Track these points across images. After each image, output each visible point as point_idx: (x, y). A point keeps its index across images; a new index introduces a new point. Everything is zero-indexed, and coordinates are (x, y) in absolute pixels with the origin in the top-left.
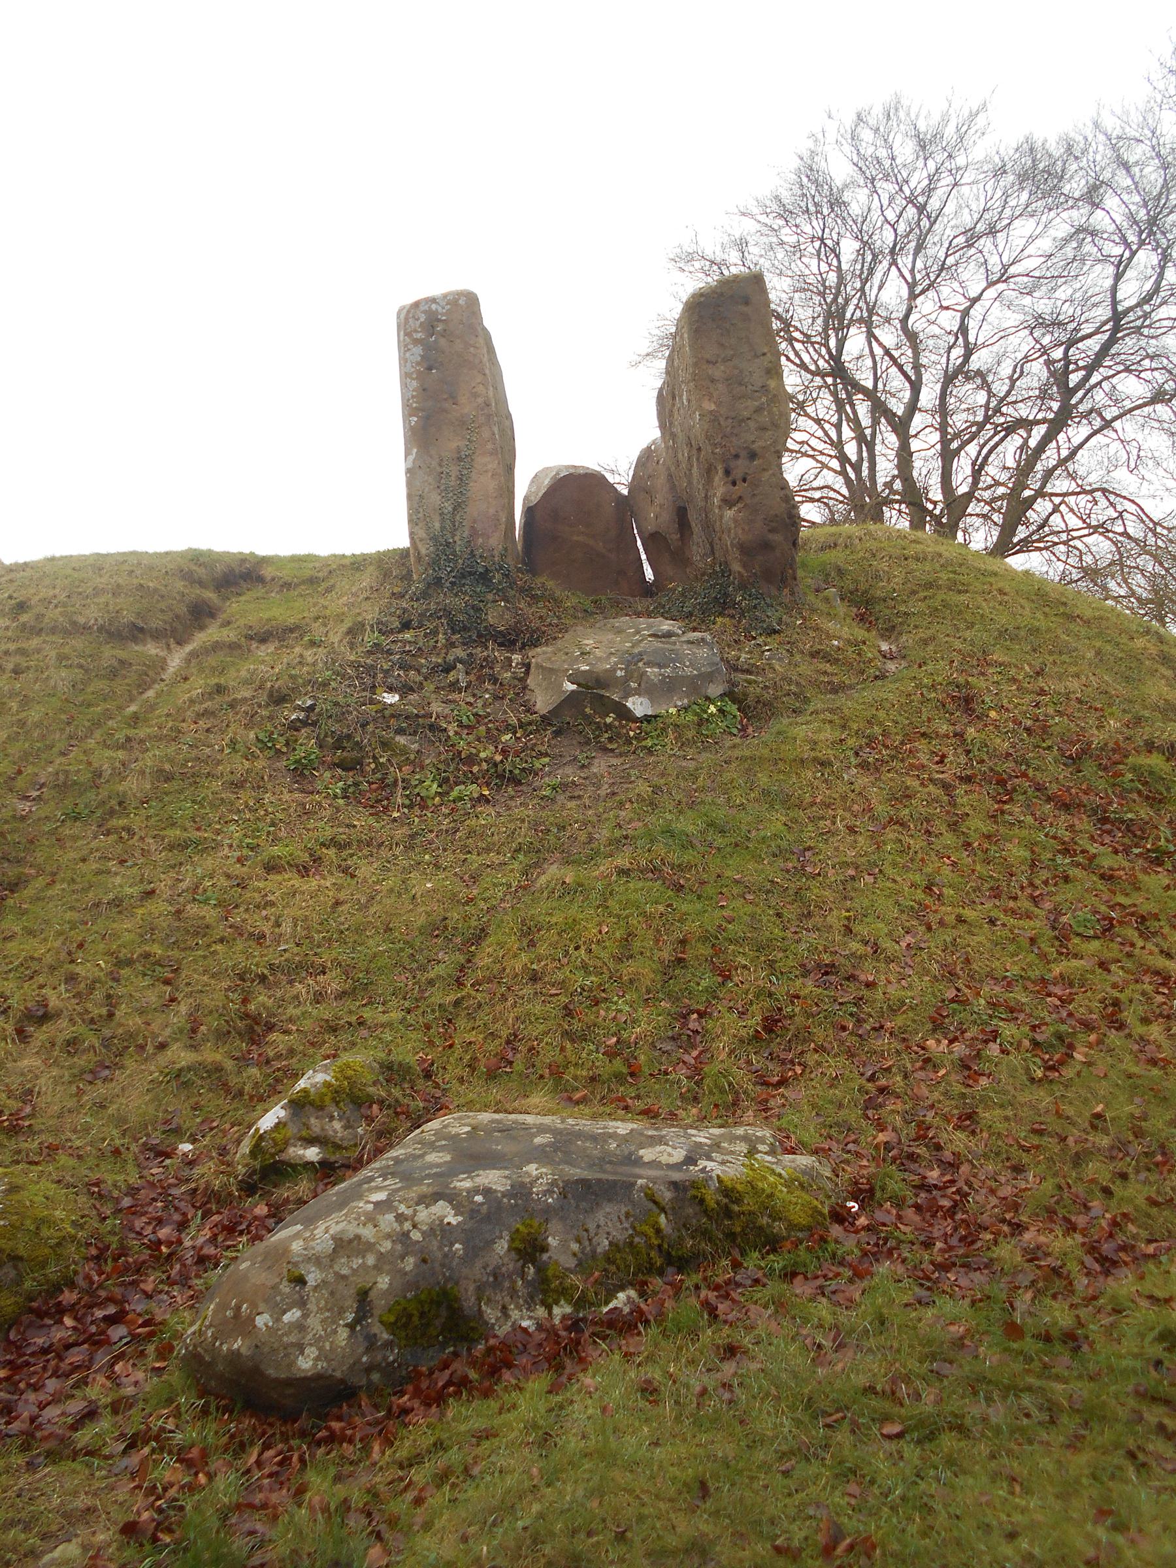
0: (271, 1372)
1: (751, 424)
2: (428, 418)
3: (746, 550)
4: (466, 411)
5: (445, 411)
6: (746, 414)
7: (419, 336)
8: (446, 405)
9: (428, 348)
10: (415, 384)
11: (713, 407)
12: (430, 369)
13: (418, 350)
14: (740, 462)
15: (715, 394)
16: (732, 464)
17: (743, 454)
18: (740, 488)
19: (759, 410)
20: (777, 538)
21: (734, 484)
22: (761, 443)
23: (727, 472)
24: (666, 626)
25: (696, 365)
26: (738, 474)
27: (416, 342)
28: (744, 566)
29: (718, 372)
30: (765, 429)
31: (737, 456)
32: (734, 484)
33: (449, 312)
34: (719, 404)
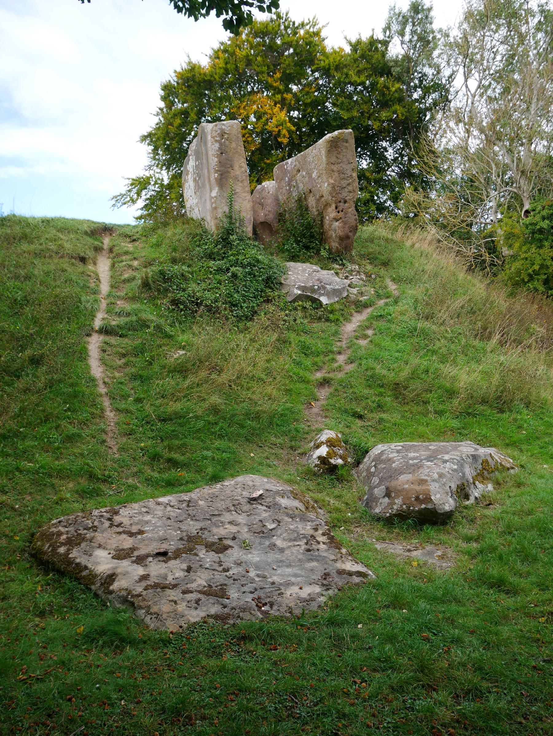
0: (439, 511)
1: (346, 190)
2: (221, 175)
3: (341, 239)
4: (238, 173)
5: (229, 172)
6: (344, 186)
7: (218, 139)
8: (230, 170)
9: (221, 144)
10: (216, 159)
11: (333, 182)
12: (222, 153)
13: (217, 145)
14: (341, 204)
15: (334, 177)
16: (339, 204)
17: (342, 201)
18: (341, 214)
19: (349, 184)
20: (351, 234)
21: (338, 212)
22: (349, 197)
23: (336, 208)
24: (315, 267)
25: (327, 164)
26: (340, 208)
27: (216, 141)
28: (340, 245)
29: (335, 168)
30: (350, 192)
31: (340, 202)
32: (338, 212)
33: (230, 130)
34: (335, 181)
